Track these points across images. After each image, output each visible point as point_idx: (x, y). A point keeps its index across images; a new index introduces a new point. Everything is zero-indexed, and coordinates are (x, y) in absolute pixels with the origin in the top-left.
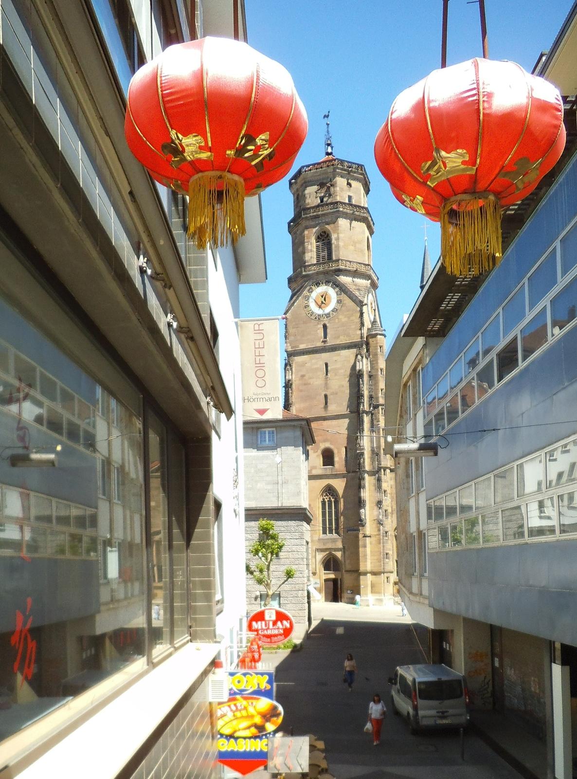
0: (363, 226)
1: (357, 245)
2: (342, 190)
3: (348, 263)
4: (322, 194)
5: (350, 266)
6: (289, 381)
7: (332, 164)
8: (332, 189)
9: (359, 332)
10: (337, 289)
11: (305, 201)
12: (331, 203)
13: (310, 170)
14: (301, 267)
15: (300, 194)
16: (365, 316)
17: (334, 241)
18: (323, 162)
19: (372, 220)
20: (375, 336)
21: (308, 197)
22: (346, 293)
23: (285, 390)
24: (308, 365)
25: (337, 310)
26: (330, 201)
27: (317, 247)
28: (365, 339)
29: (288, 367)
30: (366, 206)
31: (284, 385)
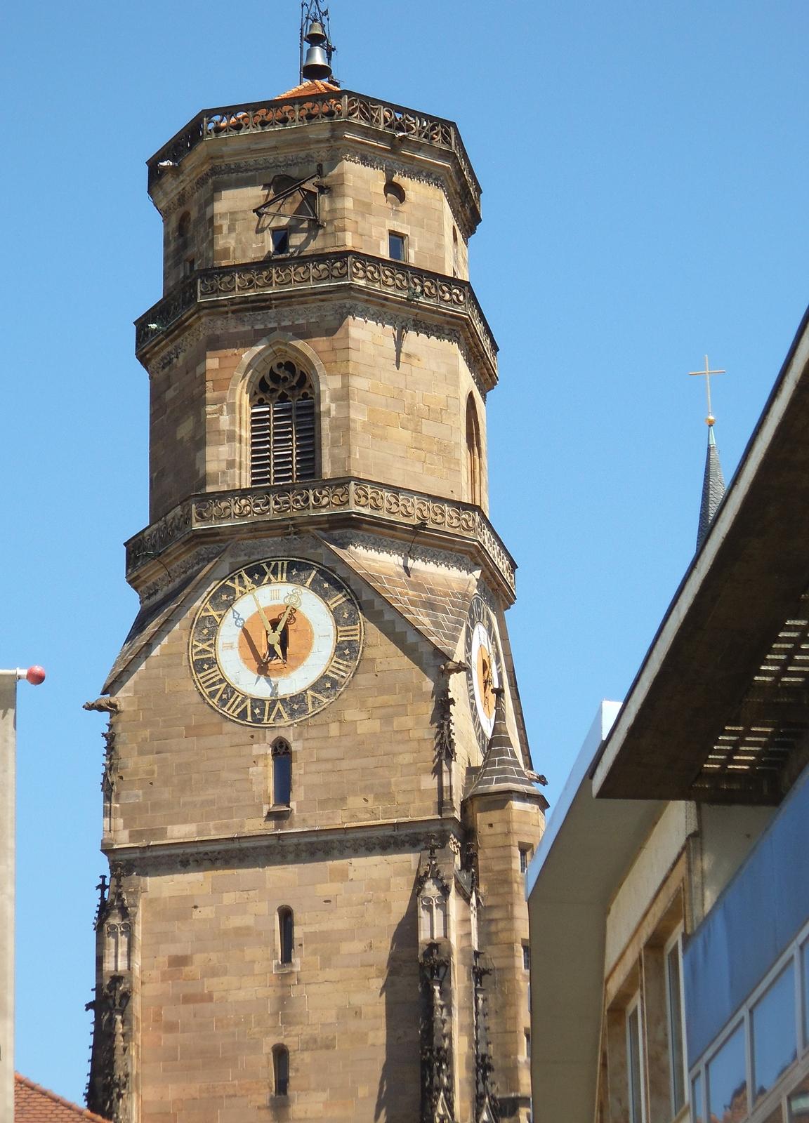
0: (452, 352)
1: (428, 428)
2: (365, 208)
3: (387, 494)
4: (285, 221)
5: (394, 508)
6: (117, 979)
7: (326, 109)
8: (324, 203)
9: (430, 782)
10: (339, 599)
11: (212, 243)
12: (321, 257)
13: (238, 127)
14: (185, 501)
15: (194, 214)
16: (459, 714)
17: (326, 403)
18: (291, 101)
19: (488, 331)
20: (500, 800)
21: (225, 229)
22: (375, 616)
23: (97, 1023)
24: (205, 913)
25: (335, 684)
26: (314, 246)
27: (258, 422)
28: (457, 815)
29: (115, 920)
30: (463, 275)
31: (92, 997)
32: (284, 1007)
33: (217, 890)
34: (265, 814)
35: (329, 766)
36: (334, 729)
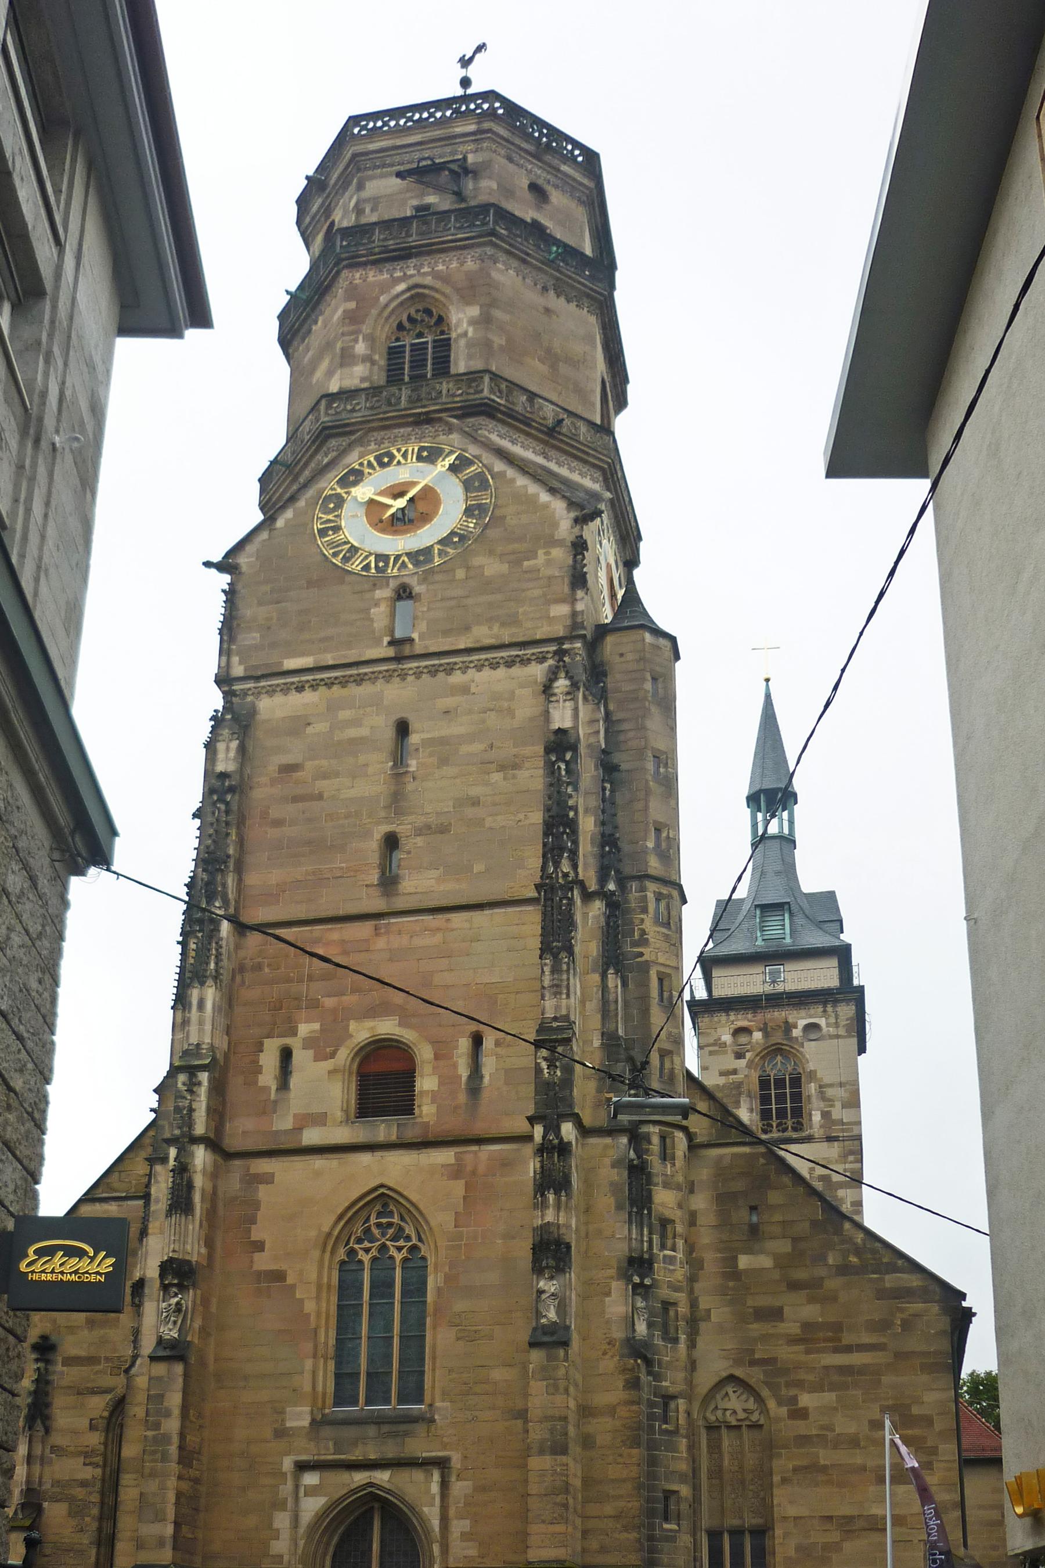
24: (320, 727)
32: (397, 801)
33: (332, 707)
34: (385, 643)
35: (453, 603)
36: (460, 574)
